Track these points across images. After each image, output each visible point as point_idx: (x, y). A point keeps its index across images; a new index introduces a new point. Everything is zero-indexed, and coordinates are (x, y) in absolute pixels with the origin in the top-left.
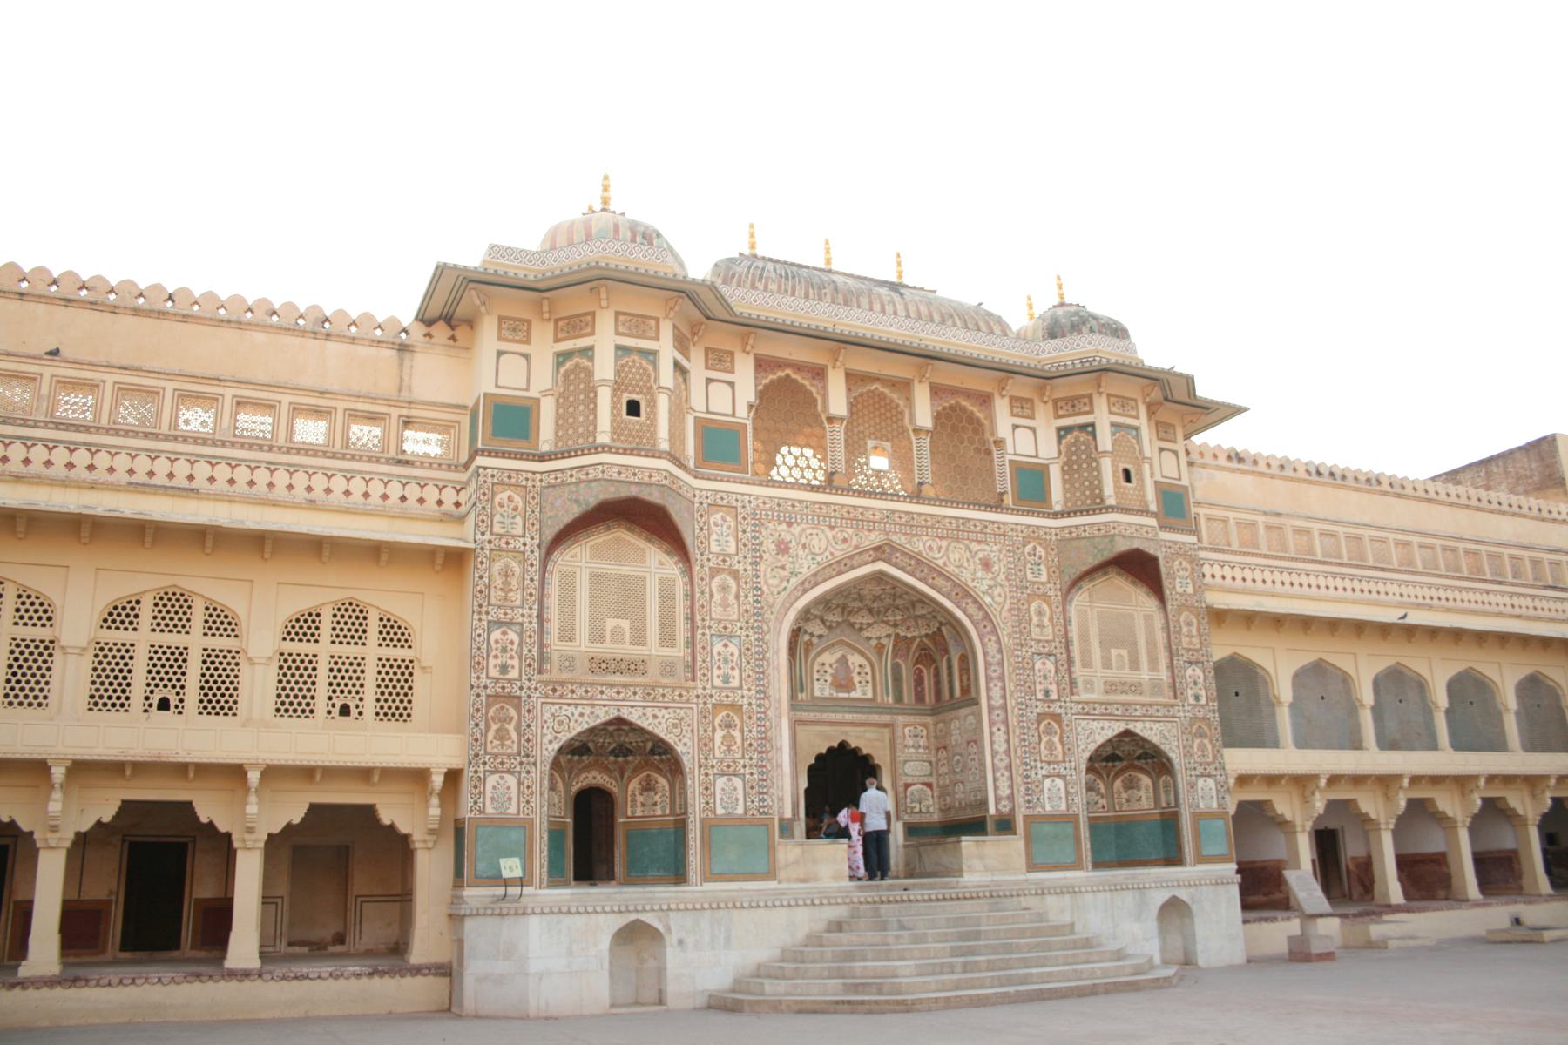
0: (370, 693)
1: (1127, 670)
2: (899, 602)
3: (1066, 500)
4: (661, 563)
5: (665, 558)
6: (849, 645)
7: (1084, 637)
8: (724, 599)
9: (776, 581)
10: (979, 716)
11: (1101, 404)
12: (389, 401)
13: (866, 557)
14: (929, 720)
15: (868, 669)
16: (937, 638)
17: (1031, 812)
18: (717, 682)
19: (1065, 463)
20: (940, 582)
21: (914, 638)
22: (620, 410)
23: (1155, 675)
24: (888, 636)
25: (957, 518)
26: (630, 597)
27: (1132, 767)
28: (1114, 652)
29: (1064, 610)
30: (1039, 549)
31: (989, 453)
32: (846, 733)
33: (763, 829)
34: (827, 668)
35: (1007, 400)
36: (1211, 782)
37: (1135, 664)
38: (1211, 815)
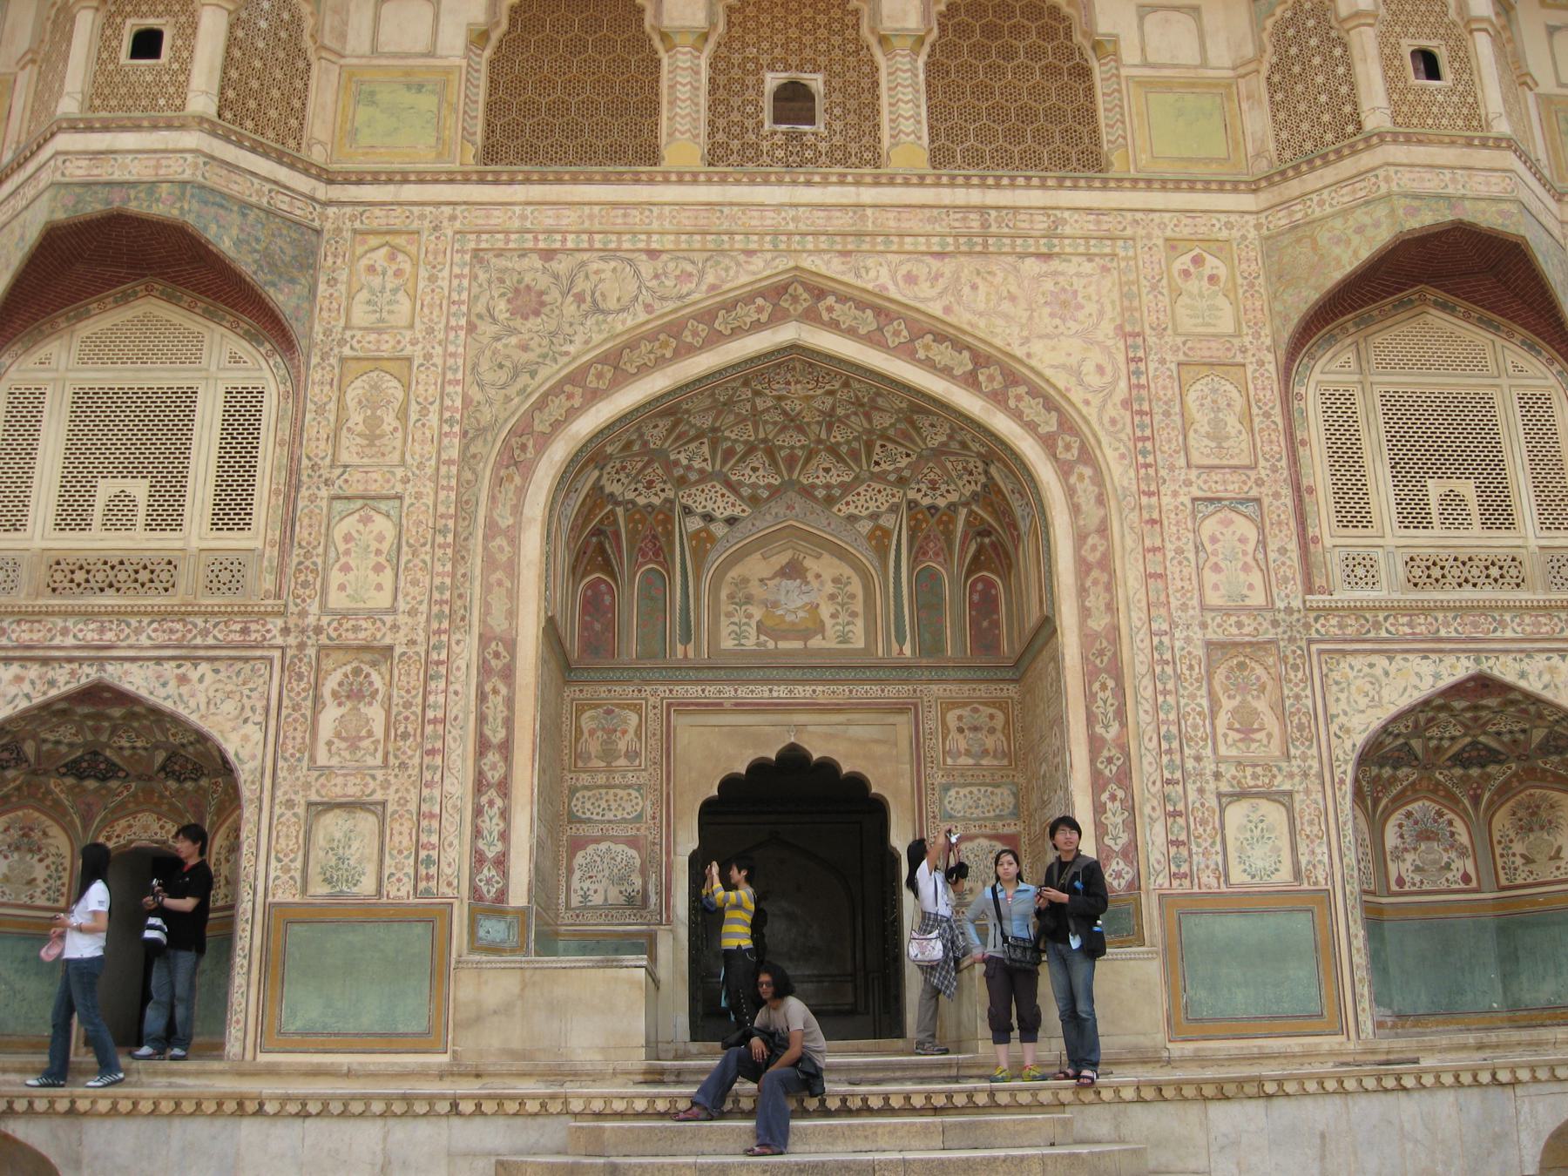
1: (1477, 528)
2: (882, 421)
3: (1281, 146)
4: (235, 359)
5: (243, 347)
6: (809, 537)
7: (1345, 455)
8: (373, 423)
10: (1057, 659)
13: (749, 314)
14: (1011, 691)
15: (856, 587)
16: (989, 494)
17: (1180, 887)
18: (336, 600)
19: (1274, 68)
21: (952, 506)
22: (115, 52)
24: (894, 509)
25: (982, 209)
27: (1532, 775)
30: (1210, 261)
31: (1084, 73)
32: (800, 727)
33: (419, 929)
34: (755, 589)
37: (1498, 514)
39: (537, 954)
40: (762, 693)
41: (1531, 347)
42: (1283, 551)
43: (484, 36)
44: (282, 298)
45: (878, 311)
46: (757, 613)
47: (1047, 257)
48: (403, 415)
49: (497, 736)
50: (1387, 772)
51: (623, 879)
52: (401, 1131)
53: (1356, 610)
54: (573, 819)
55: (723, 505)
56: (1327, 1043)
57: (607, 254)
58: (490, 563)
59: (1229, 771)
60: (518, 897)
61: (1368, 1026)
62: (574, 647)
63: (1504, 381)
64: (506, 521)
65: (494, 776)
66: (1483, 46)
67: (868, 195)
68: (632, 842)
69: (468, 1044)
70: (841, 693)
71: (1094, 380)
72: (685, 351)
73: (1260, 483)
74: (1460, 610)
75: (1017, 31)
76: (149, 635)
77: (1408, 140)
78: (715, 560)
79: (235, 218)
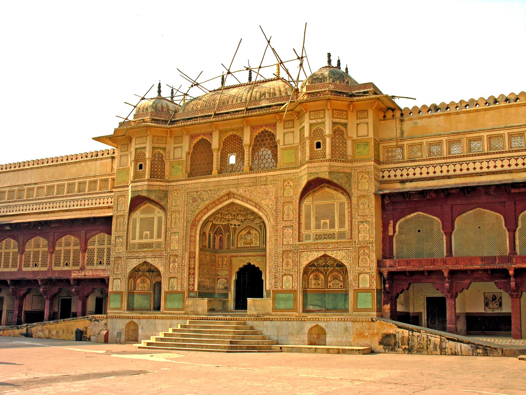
0: (105, 258)
5: (159, 210)
6: (251, 227)
7: (308, 217)
8: (176, 221)
9: (191, 213)
11: (307, 116)
12: (109, 175)
15: (258, 235)
18: (172, 248)
20: (252, 203)
23: (342, 230)
25: (256, 177)
26: (148, 224)
28: (322, 221)
29: (300, 207)
30: (290, 183)
31: (276, 147)
32: (249, 259)
33: (181, 295)
35: (282, 124)
36: (368, 276)
37: (332, 226)
38: (365, 291)
39: (199, 297)
40: (244, 254)
41: (342, 193)
42: (296, 234)
43: (189, 153)
44: (162, 203)
45: (242, 197)
46: (243, 240)
47: (265, 185)
48: (179, 220)
49: (192, 267)
50: (326, 268)
51: (224, 285)
52: (172, 321)
53: (306, 244)
54: (218, 275)
55: (237, 223)
56: (294, 313)
57: (205, 191)
58: (191, 241)
59: (284, 271)
60: (196, 289)
61: (301, 311)
62: (217, 247)
63: (337, 200)
64: (193, 234)
65: (192, 273)
66: (328, 140)
67: (240, 177)
68: (225, 279)
69: (187, 310)
70: (255, 254)
71: (270, 207)
72: (217, 205)
73: (293, 223)
74: (323, 244)
75: (267, 140)
76: (151, 254)
77: (311, 162)
78: (237, 232)
79: (154, 193)
